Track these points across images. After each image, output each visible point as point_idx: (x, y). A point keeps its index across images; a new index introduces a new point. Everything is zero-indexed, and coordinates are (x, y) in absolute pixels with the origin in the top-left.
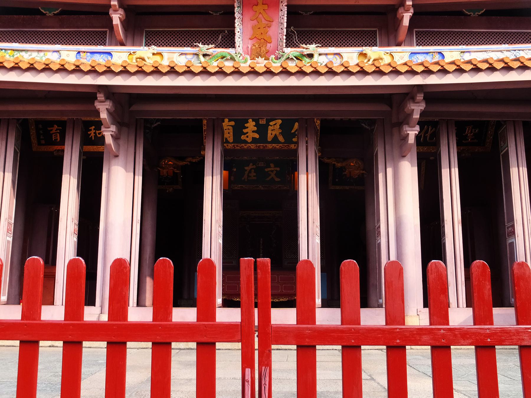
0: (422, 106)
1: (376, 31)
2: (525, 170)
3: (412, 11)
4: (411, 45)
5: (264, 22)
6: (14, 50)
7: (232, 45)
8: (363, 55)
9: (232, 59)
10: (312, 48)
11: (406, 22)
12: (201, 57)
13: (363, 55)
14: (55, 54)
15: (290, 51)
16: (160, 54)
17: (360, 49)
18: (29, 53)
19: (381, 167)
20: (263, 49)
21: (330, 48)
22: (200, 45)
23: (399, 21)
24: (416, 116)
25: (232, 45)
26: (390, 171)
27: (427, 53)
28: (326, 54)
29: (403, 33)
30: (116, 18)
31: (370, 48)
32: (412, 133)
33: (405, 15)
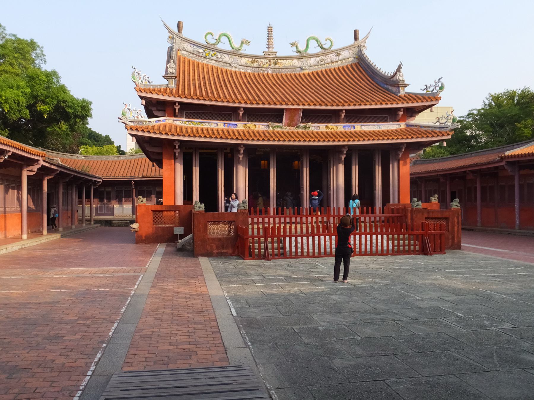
0: (347, 150)
1: (331, 115)
2: (381, 167)
3: (345, 113)
4: (344, 123)
5: (293, 115)
6: (199, 122)
7: (281, 122)
8: (327, 127)
9: (281, 128)
10: (309, 124)
11: (343, 117)
12: (270, 127)
13: (327, 127)
14: (215, 124)
15: (302, 125)
16: (255, 125)
17: (326, 124)
18: (205, 124)
19: (332, 166)
20: (292, 123)
21: (315, 124)
22: (270, 123)
23: (340, 116)
24: (345, 152)
25: (281, 122)
26: (335, 167)
27: (349, 126)
28: (314, 126)
29: (341, 120)
30: (241, 113)
31: (329, 124)
32: (343, 157)
33: (342, 114)
